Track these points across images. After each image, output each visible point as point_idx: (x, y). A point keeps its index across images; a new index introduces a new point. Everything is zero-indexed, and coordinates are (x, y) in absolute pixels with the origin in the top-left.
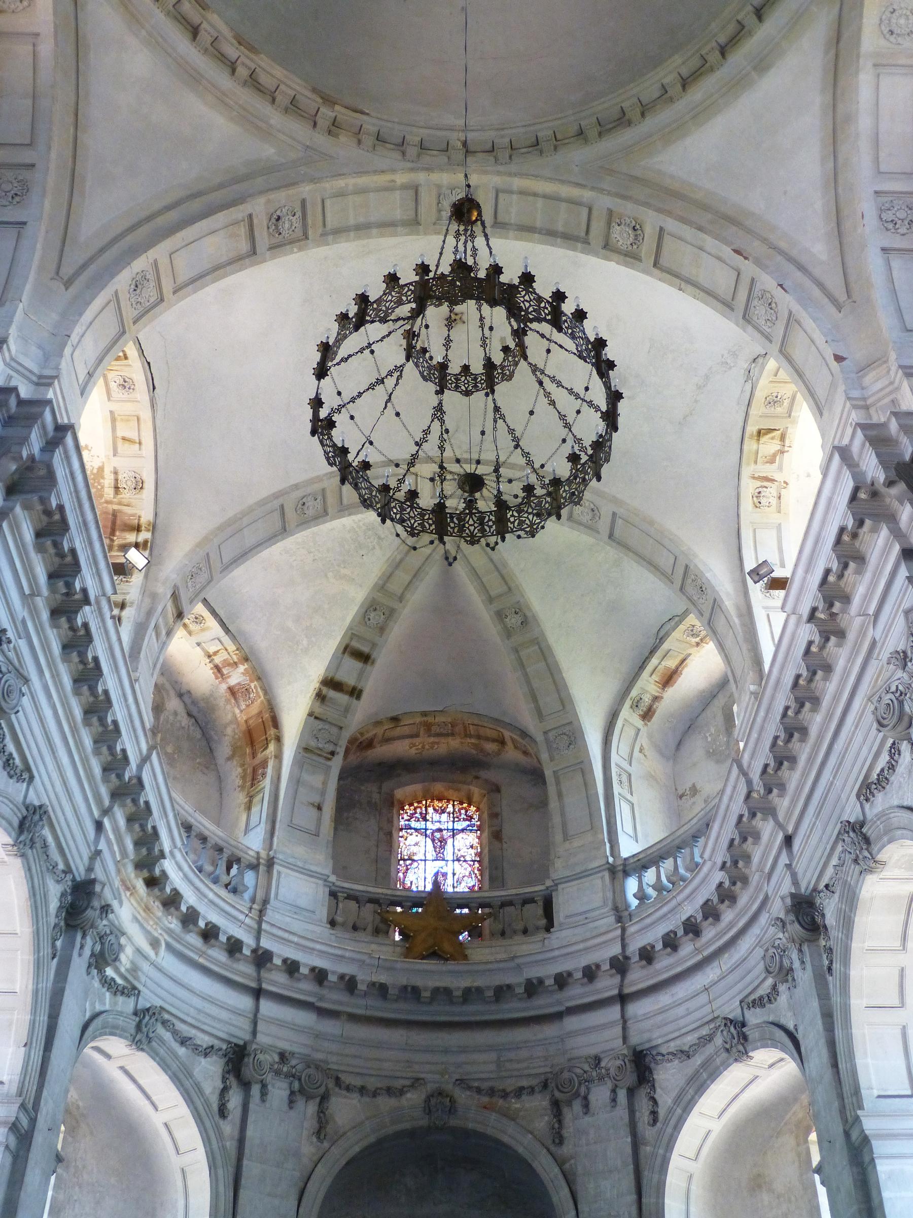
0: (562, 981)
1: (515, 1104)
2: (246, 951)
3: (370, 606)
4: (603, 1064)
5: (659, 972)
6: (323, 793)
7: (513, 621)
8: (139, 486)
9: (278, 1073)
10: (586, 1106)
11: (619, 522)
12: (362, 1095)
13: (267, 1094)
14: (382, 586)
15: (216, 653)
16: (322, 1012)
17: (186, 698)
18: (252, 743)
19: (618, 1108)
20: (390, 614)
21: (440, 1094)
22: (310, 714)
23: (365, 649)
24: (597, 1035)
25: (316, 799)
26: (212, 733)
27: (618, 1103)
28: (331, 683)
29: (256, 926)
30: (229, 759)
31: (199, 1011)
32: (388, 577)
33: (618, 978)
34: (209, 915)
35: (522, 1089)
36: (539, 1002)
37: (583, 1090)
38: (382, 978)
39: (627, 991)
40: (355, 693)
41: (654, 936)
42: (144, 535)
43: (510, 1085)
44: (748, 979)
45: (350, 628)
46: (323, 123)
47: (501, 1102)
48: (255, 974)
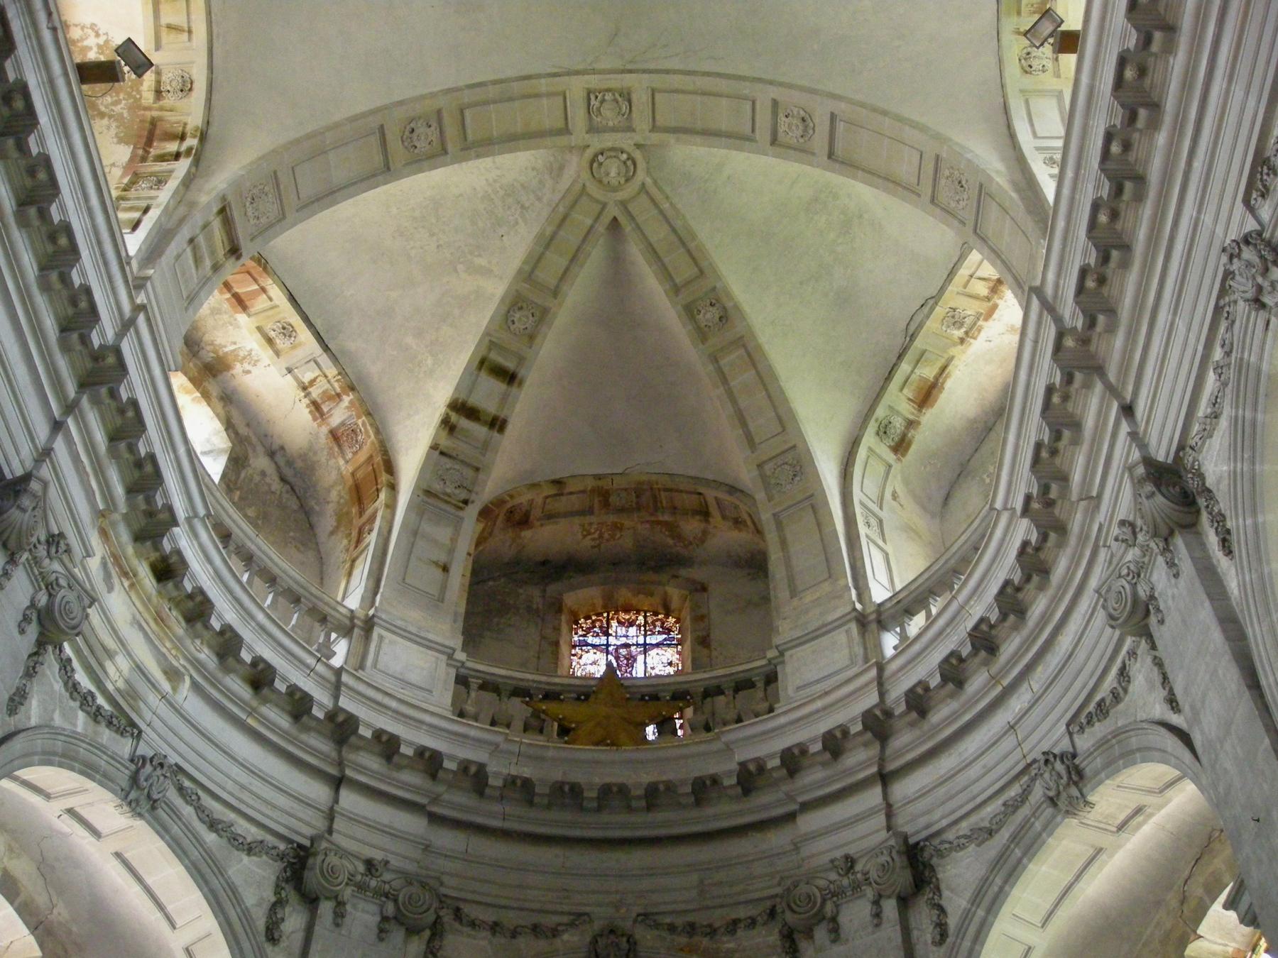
2: (318, 713)
3: (515, 303)
4: (858, 867)
5: (938, 728)
6: (451, 551)
7: (708, 316)
8: (186, 87)
9: (362, 887)
10: (835, 931)
11: (841, 127)
12: (494, 933)
13: (343, 916)
14: (528, 274)
15: (312, 382)
16: (434, 819)
17: (279, 458)
19: (883, 926)
20: (543, 315)
21: (612, 932)
22: (434, 447)
23: (510, 365)
24: (850, 828)
25: (442, 557)
26: (313, 503)
27: (885, 918)
28: (461, 407)
29: (333, 678)
30: (332, 533)
31: (243, 787)
32: (535, 261)
33: (874, 750)
34: (257, 646)
35: (735, 922)
37: (829, 907)
38: (526, 772)
39: (891, 766)
43: (718, 917)
44: (1078, 684)
45: (487, 333)
47: (705, 942)
48: (334, 754)
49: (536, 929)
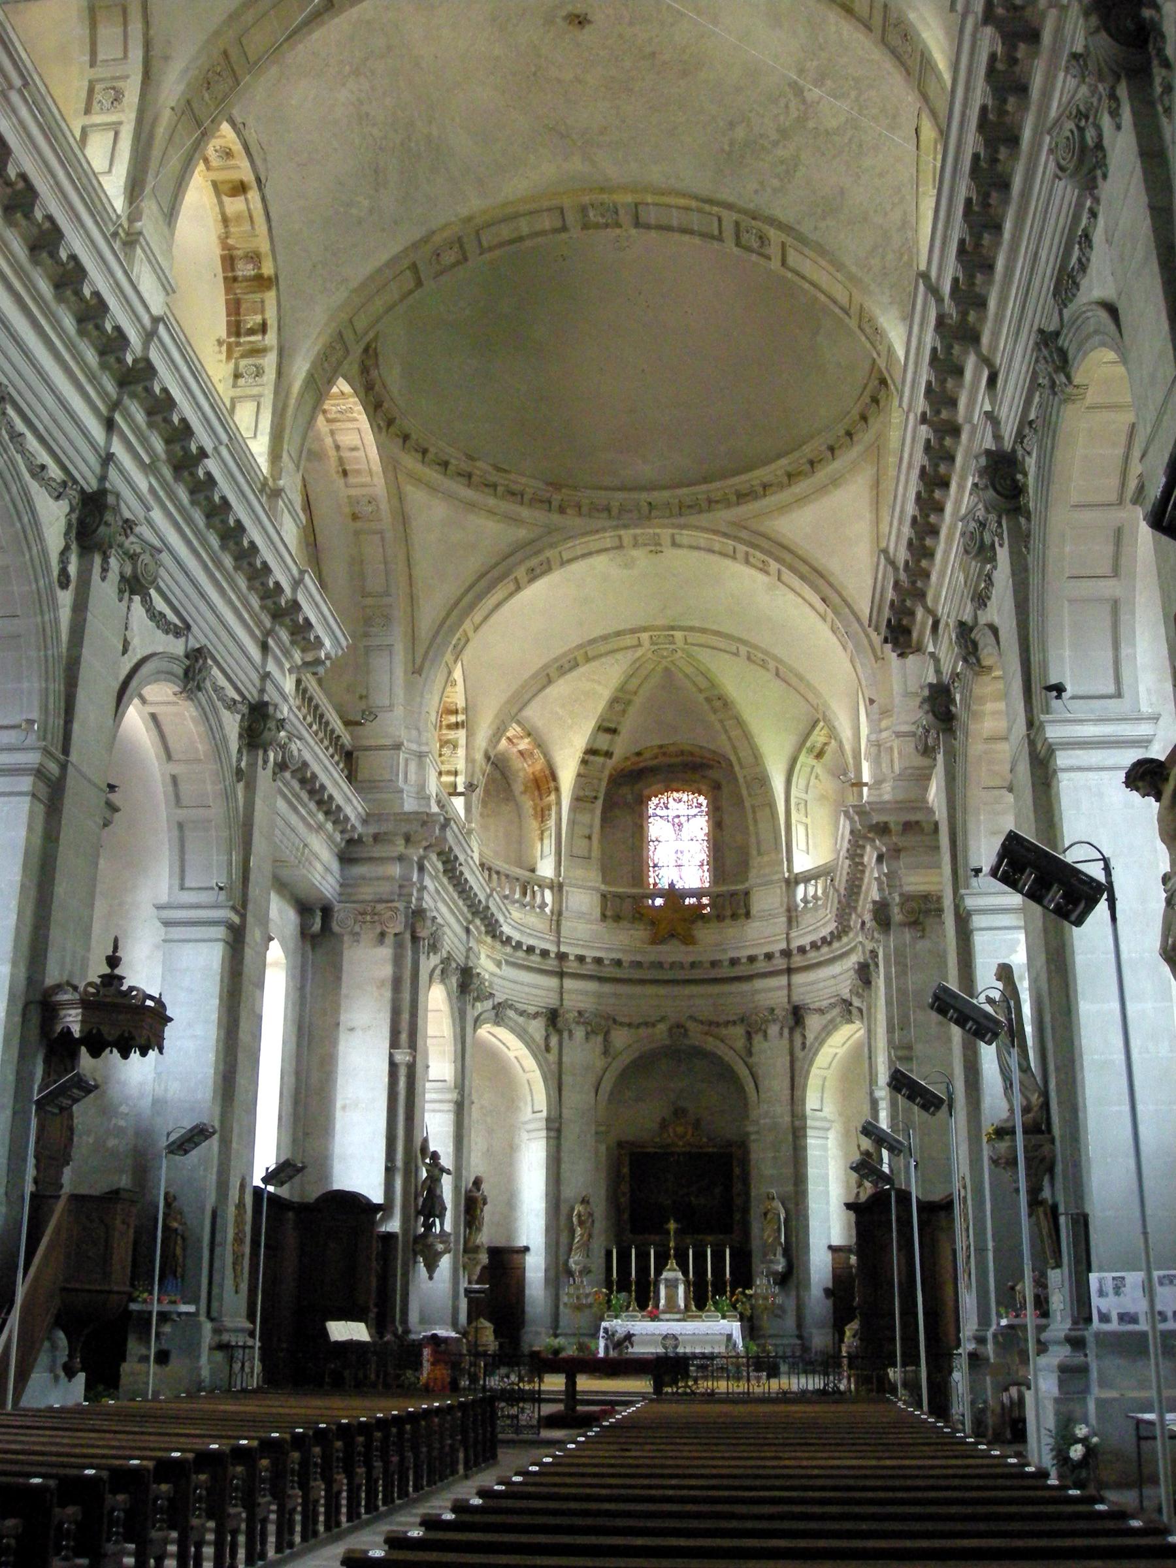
0: (752, 959)
1: (724, 1031)
3: (614, 701)
6: (591, 826)
9: (578, 1023)
14: (622, 688)
16: (600, 979)
18: (538, 788)
20: (629, 703)
23: (613, 726)
24: (771, 993)
25: (587, 832)
28: (591, 751)
36: (740, 972)
38: (639, 958)
40: (608, 754)
41: (805, 941)
42: (461, 718)
43: (722, 1018)
46: (555, 504)
49: (646, 1024)
